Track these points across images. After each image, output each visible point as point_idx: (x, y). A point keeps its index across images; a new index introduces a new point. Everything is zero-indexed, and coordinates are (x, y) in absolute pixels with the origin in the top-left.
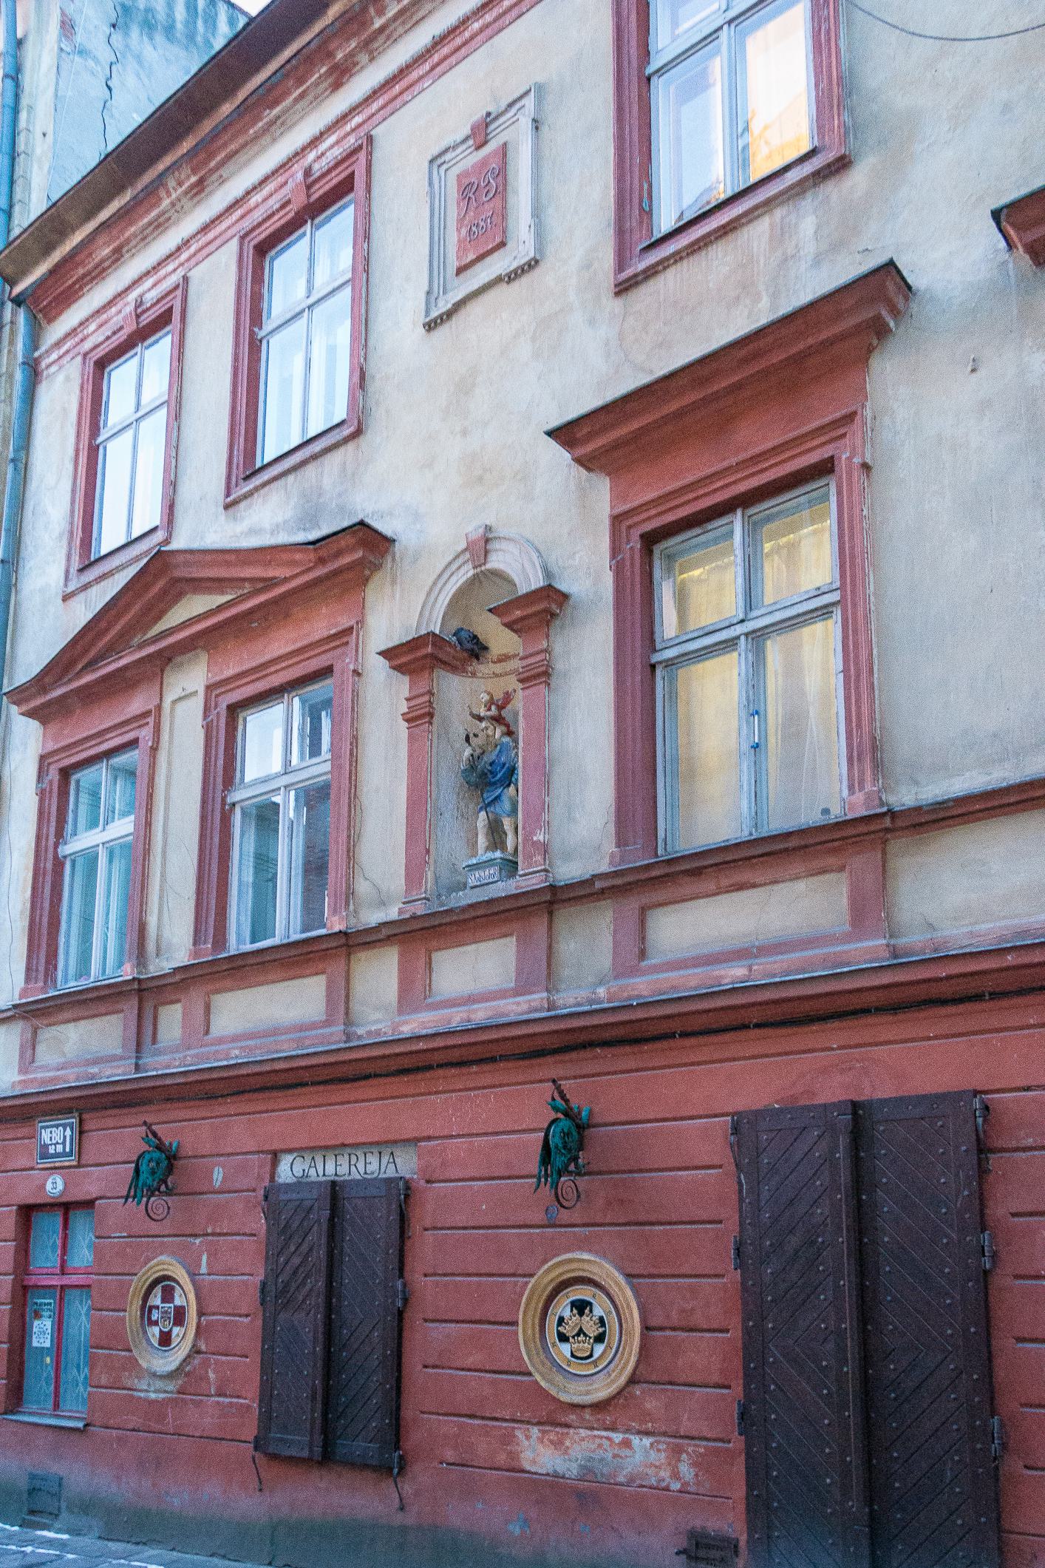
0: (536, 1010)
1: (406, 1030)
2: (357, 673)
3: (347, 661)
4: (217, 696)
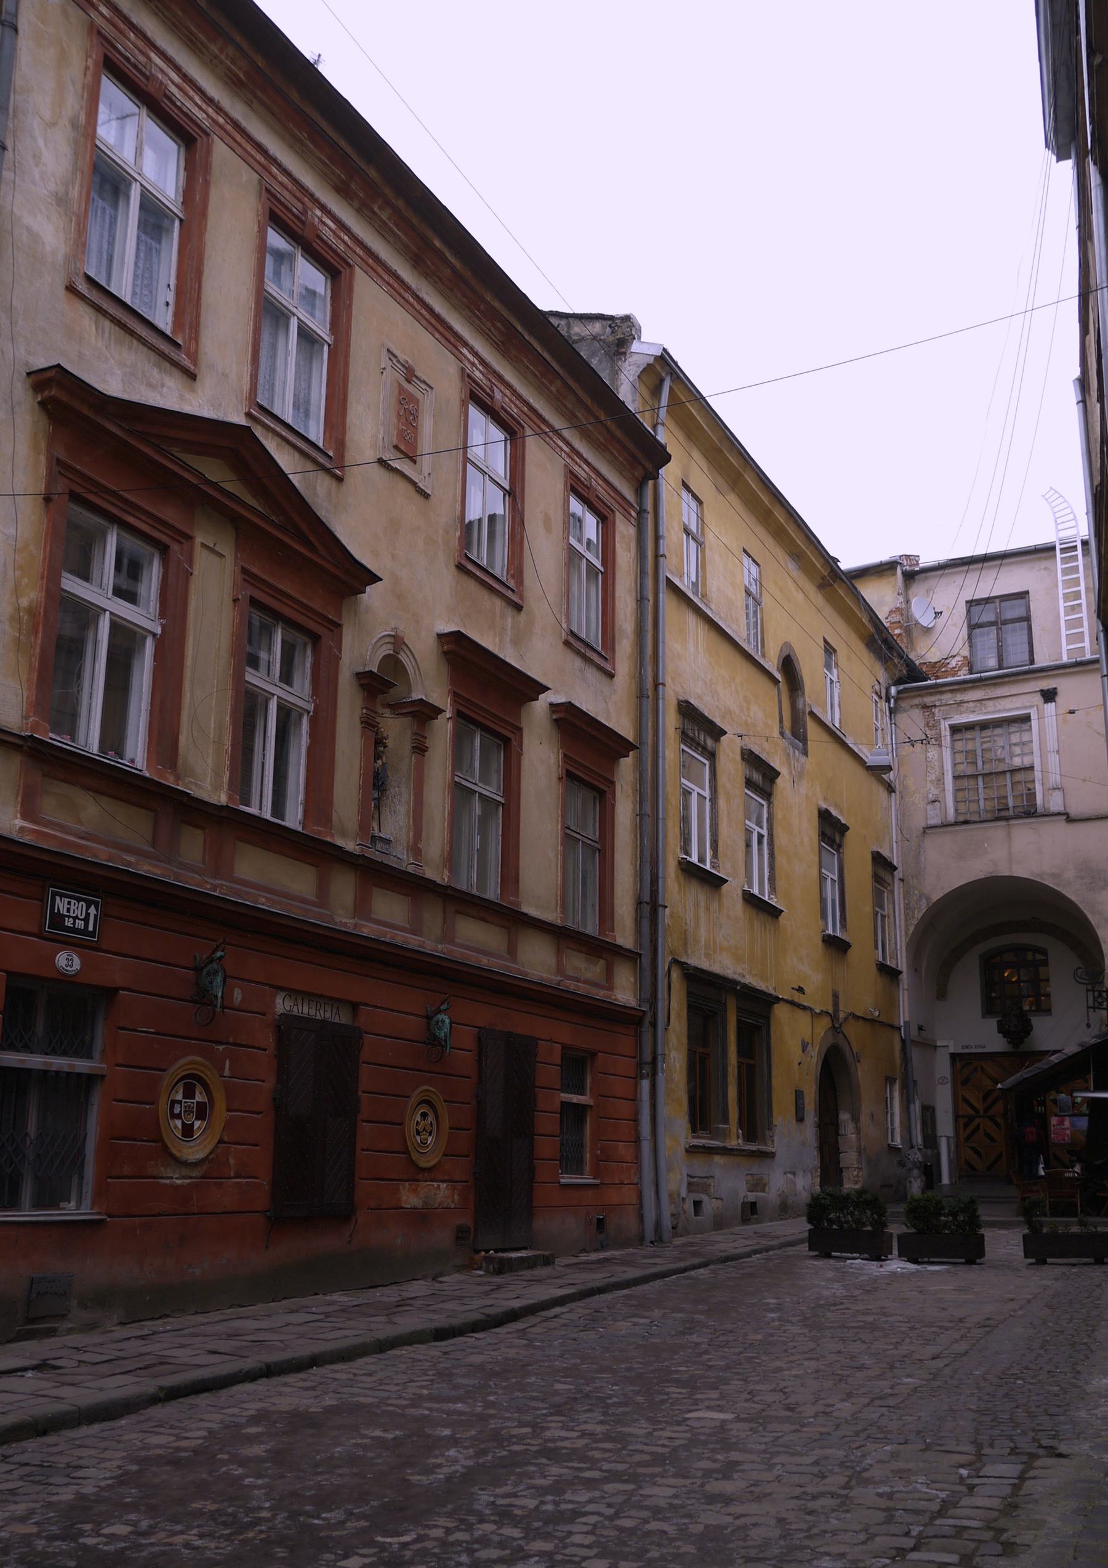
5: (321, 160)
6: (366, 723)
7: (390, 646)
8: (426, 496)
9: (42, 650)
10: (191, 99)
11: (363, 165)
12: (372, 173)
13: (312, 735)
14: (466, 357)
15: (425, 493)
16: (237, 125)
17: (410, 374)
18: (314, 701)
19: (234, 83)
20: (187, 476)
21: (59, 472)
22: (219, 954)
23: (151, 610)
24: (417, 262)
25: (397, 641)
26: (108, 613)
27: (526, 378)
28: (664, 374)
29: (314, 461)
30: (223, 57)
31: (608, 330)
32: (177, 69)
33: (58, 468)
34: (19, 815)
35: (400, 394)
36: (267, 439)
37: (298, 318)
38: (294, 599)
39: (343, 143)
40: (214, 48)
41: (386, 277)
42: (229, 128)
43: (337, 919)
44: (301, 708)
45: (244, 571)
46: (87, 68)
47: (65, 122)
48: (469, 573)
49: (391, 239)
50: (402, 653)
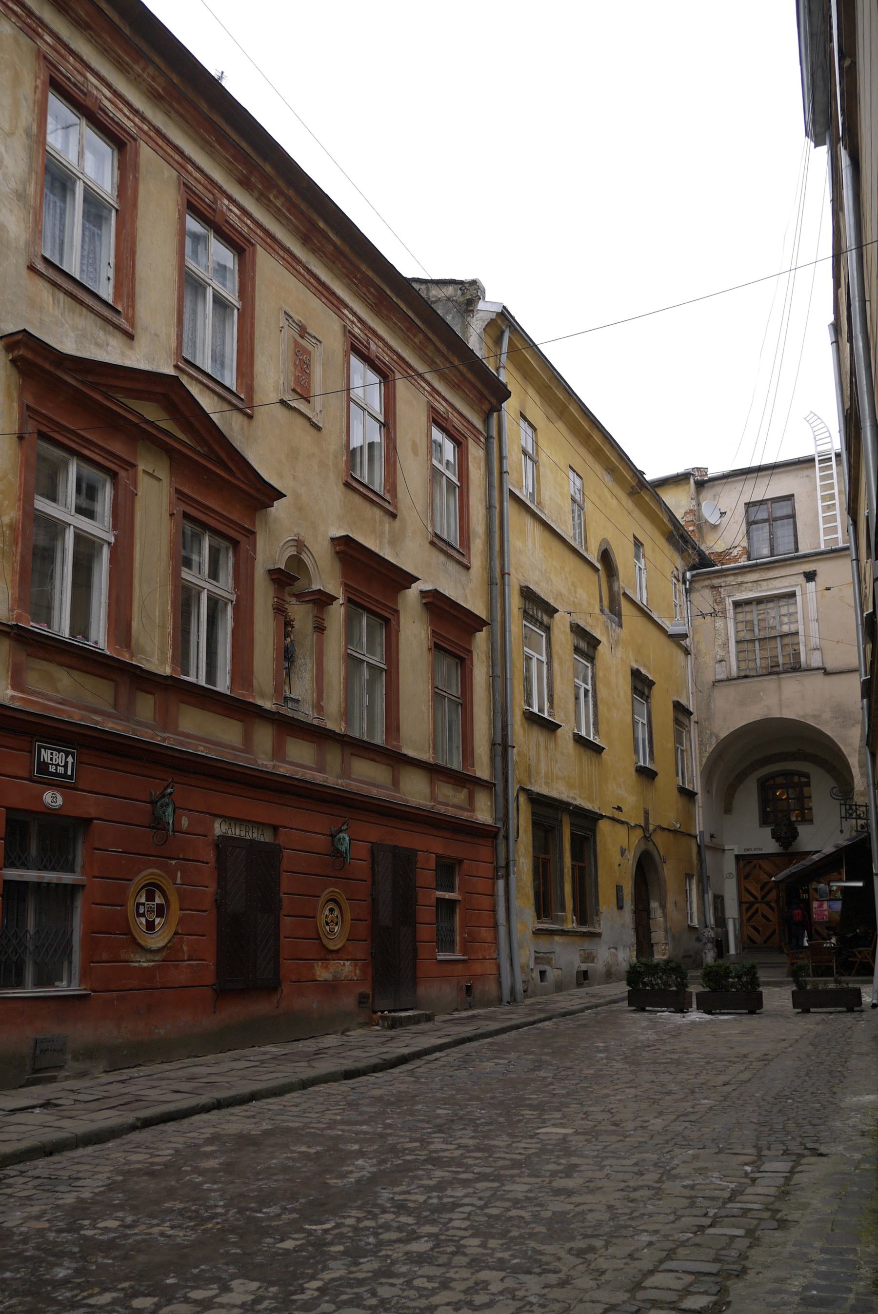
5: (227, 159)
6: (277, 609)
7: (294, 548)
8: (318, 429)
9: (22, 558)
10: (121, 110)
11: (261, 162)
12: (268, 168)
13: (236, 619)
14: (347, 317)
15: (318, 426)
16: (158, 132)
17: (303, 331)
18: (236, 593)
19: (155, 97)
20: (129, 416)
21: (29, 415)
22: (169, 790)
23: (106, 524)
24: (306, 240)
25: (299, 544)
26: (72, 527)
27: (395, 332)
28: (504, 327)
29: (230, 403)
30: (145, 76)
31: (459, 292)
32: (109, 86)
33: (28, 412)
34: (10, 687)
35: (295, 348)
36: (191, 386)
37: (213, 288)
38: (218, 512)
39: (244, 145)
40: (138, 69)
41: (281, 253)
42: (152, 134)
43: (260, 762)
44: (226, 598)
45: (178, 491)
46: (36, 87)
47: (20, 132)
48: (355, 490)
49: (284, 222)
50: (304, 554)
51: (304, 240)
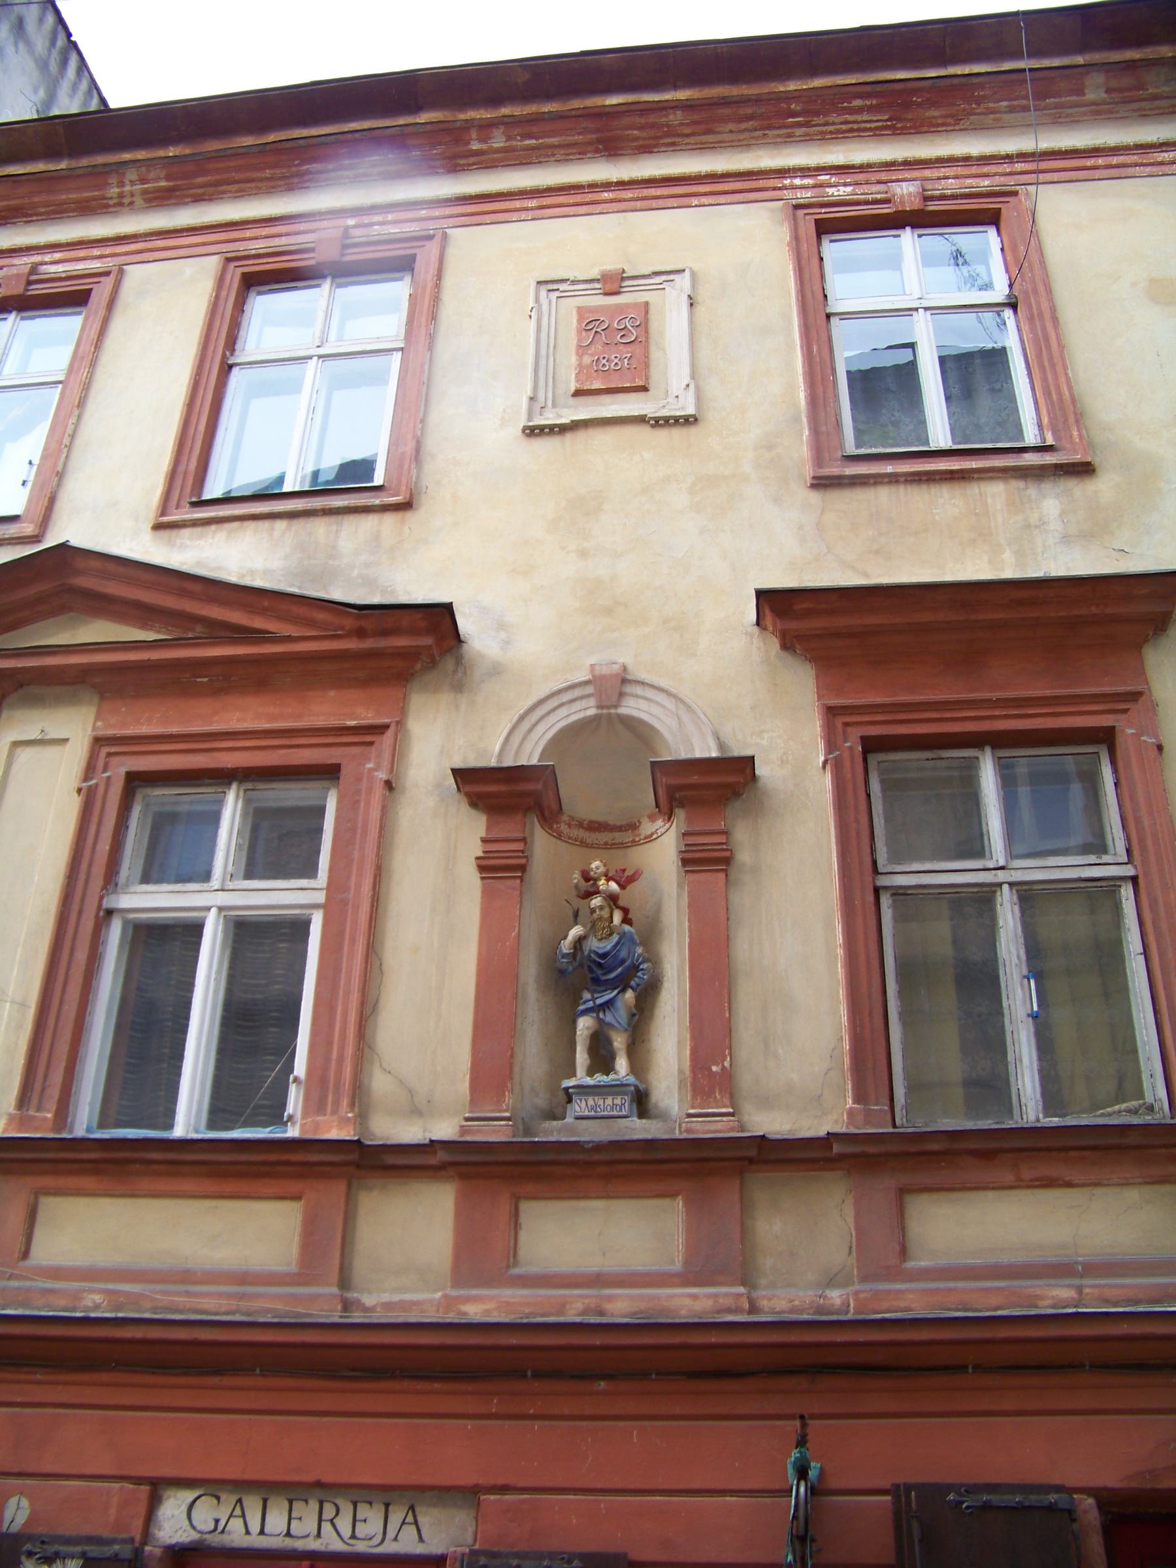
0: (729, 1310)
1: (474, 1312)
2: (389, 785)
3: (370, 765)
4: (109, 754)
8: (688, 421)
24: (611, 148)
51: (606, 149)
